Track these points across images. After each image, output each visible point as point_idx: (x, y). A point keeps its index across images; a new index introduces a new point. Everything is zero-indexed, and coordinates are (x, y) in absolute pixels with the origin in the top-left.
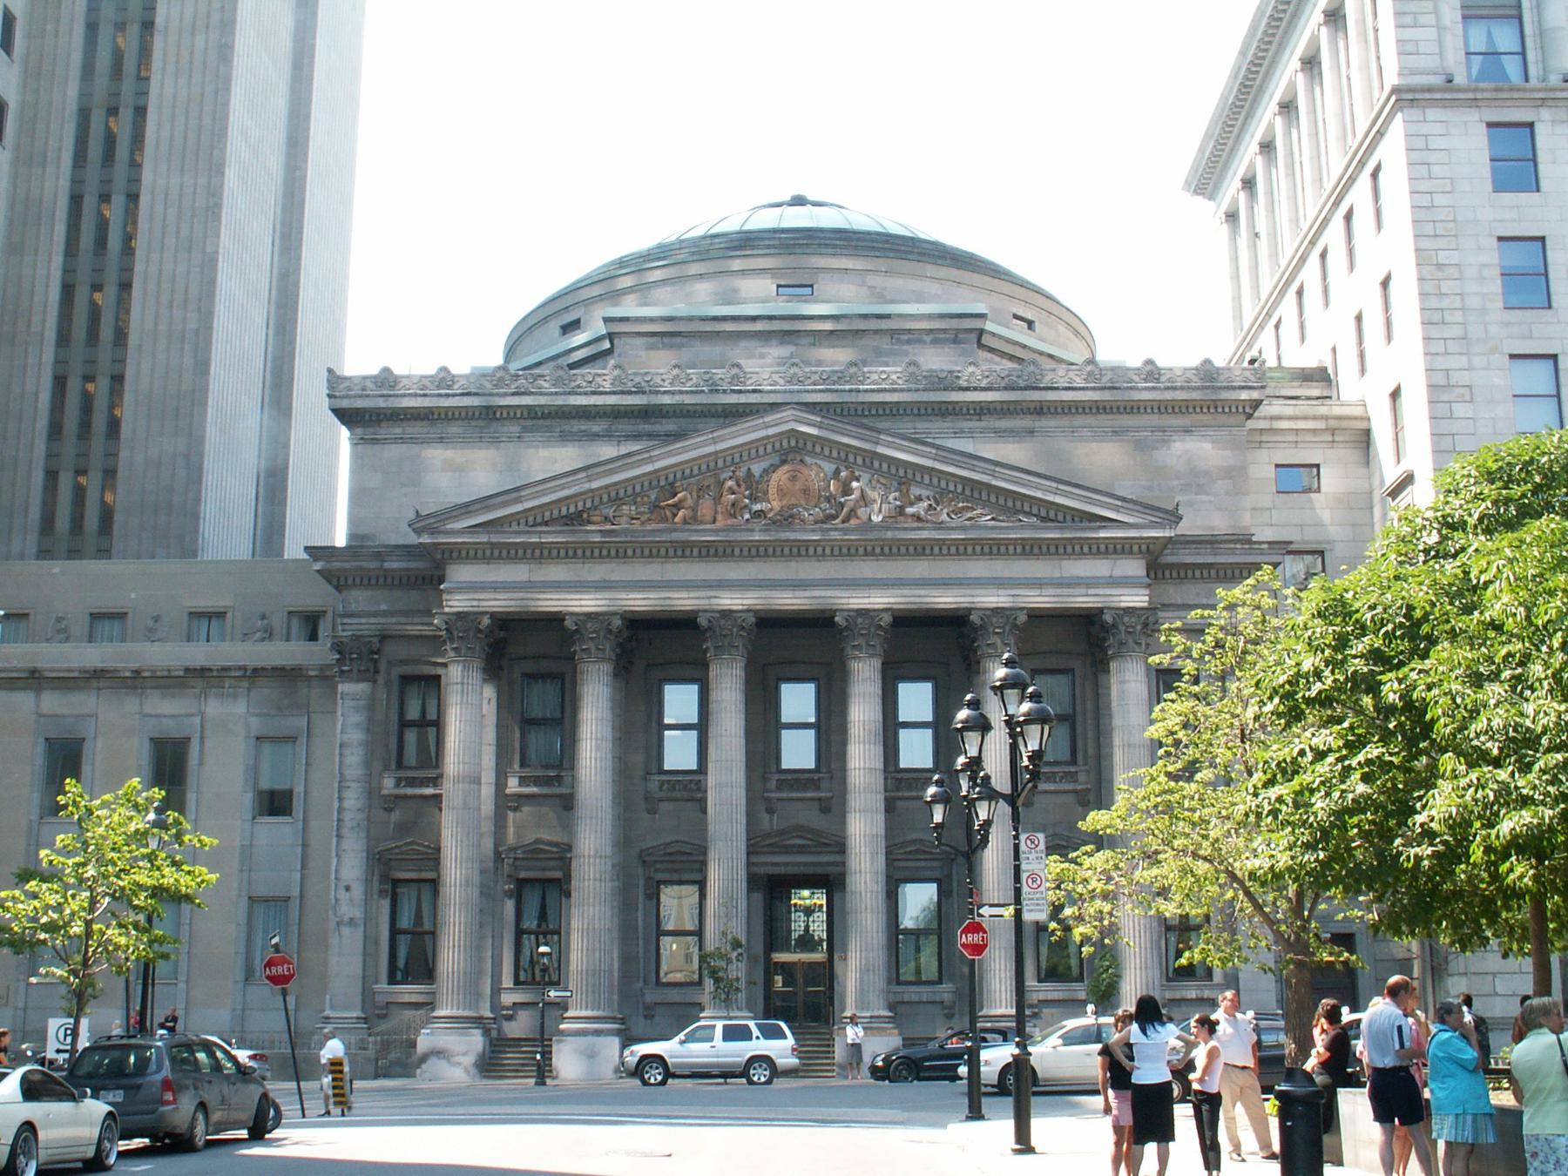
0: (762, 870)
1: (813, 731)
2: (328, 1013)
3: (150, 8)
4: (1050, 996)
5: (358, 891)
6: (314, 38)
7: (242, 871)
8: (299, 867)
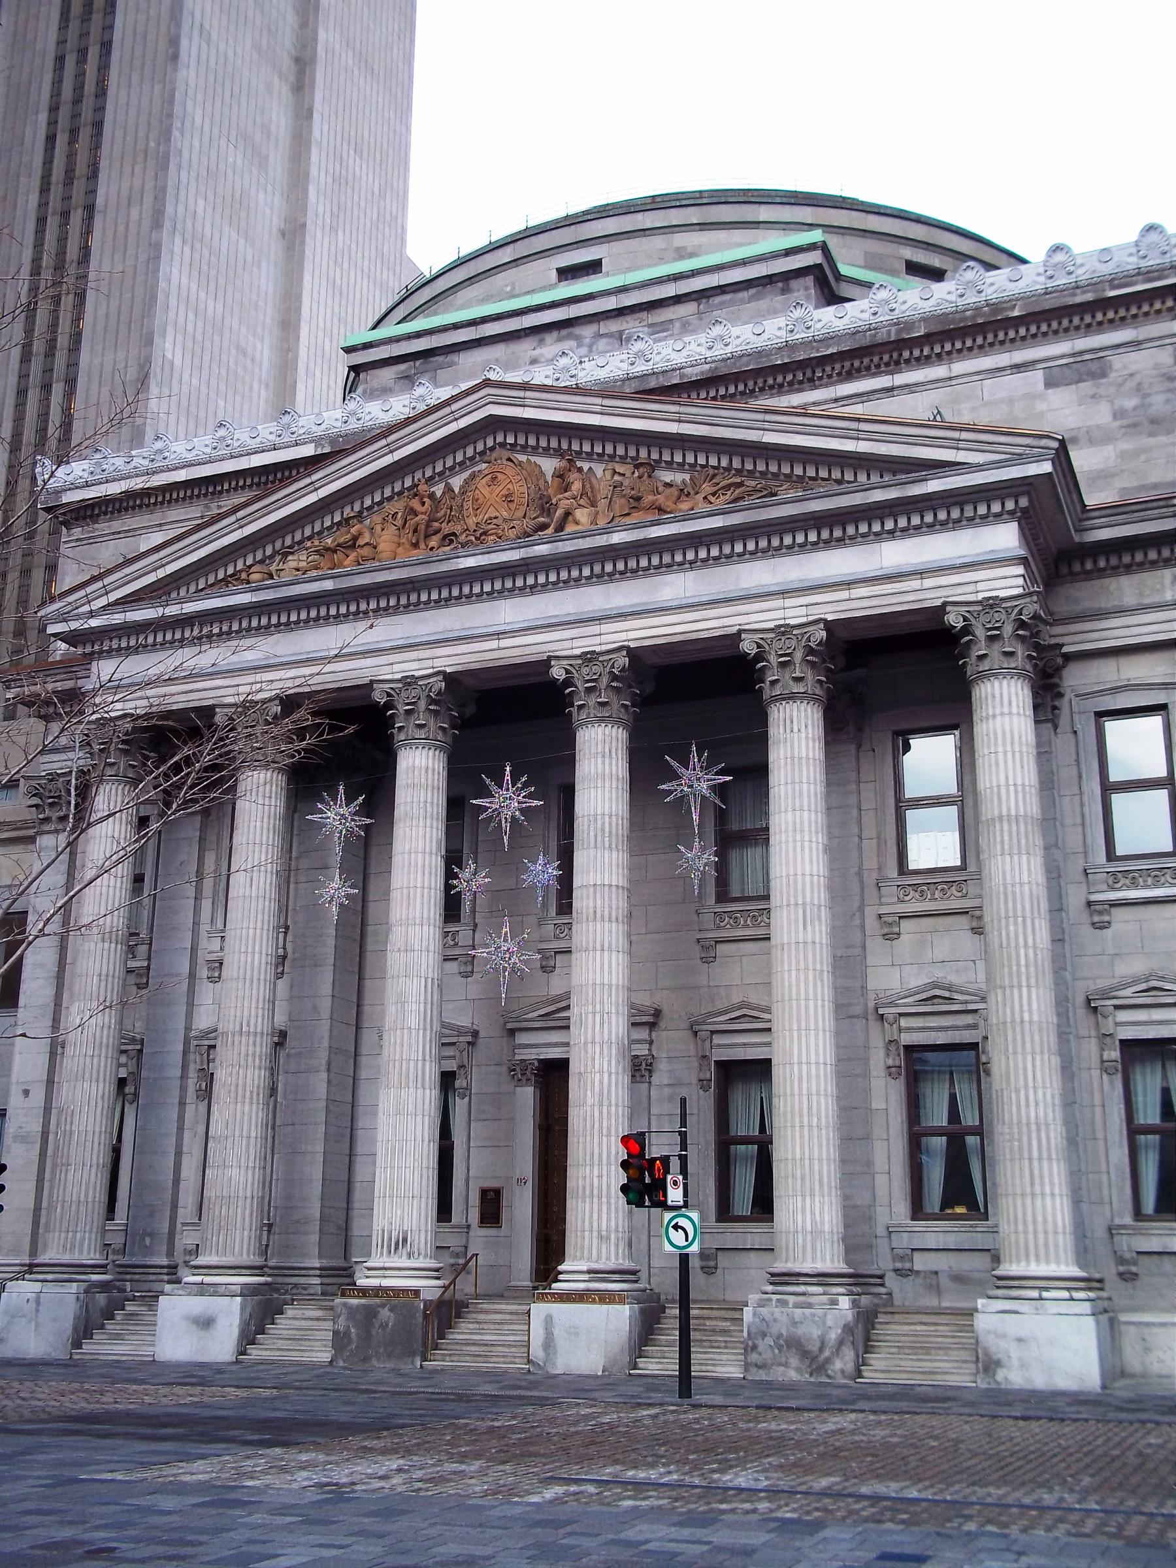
4: (931, 1241)
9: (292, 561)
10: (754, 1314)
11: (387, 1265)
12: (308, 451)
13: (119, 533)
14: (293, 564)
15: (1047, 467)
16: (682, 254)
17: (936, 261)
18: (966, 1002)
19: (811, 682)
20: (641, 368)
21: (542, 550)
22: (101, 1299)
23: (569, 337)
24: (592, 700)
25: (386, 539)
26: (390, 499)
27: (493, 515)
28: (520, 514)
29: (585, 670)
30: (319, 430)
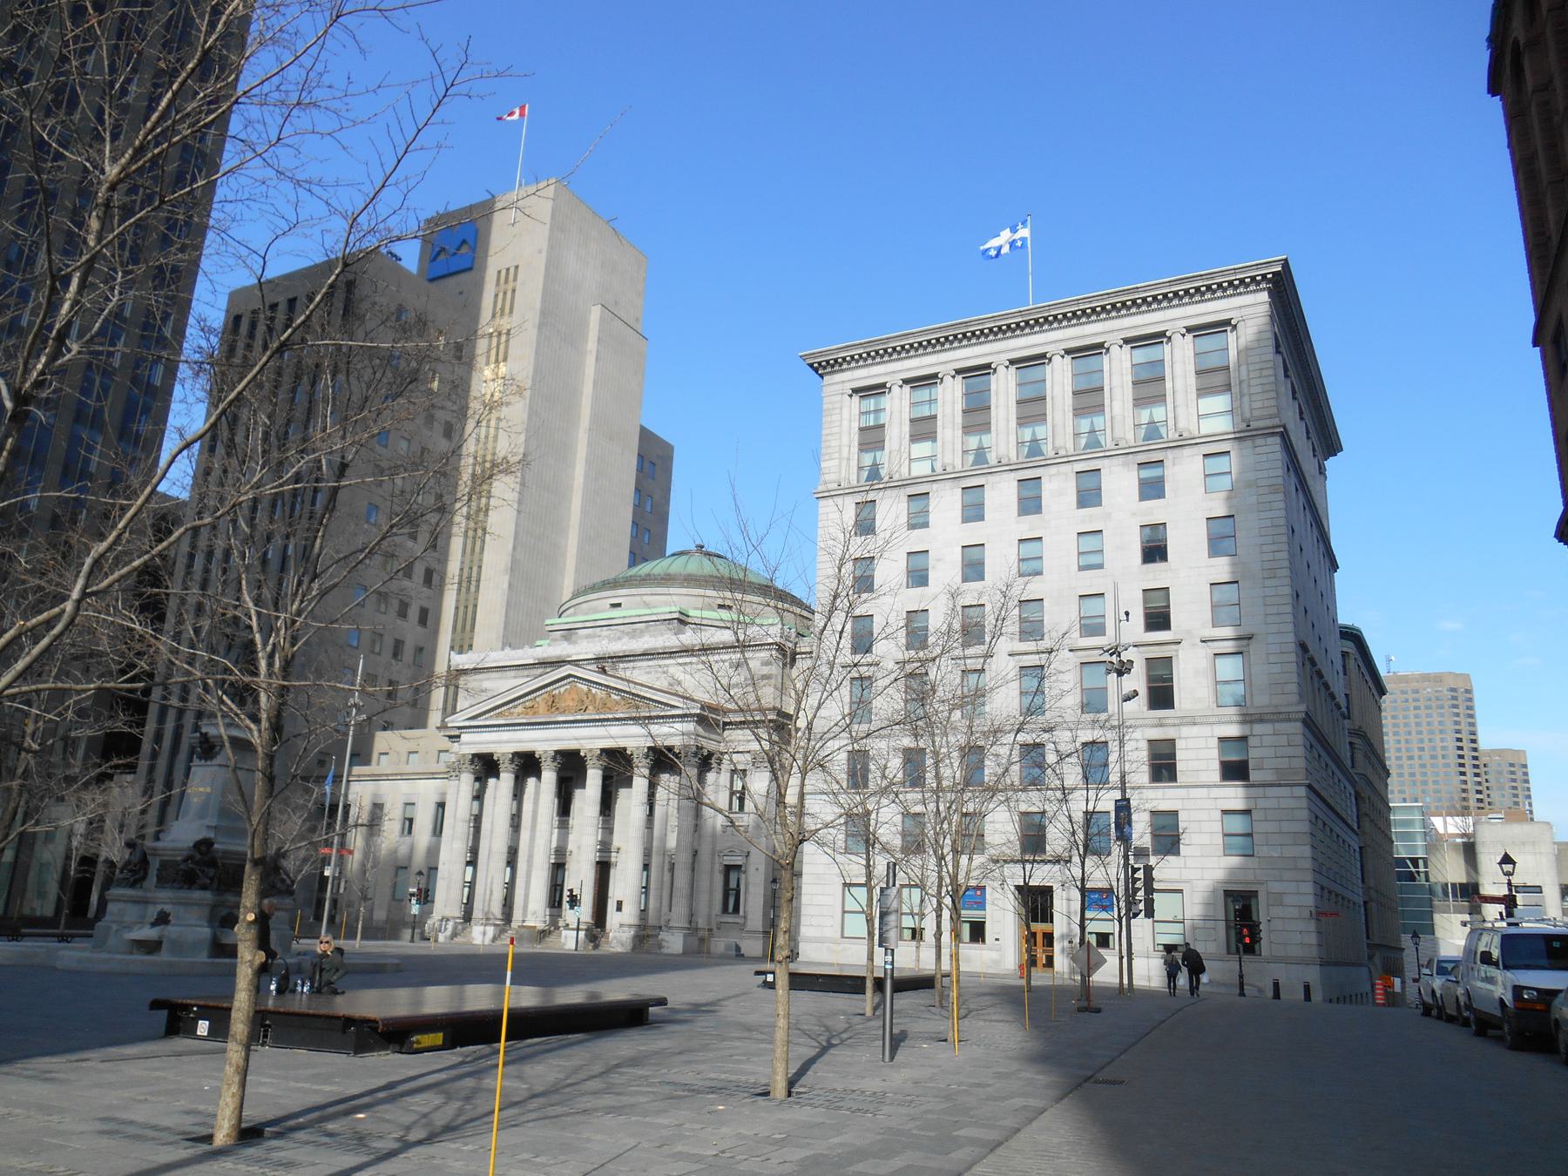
9: (516, 710)
15: (698, 711)
19: (645, 762)
20: (625, 648)
21: (579, 717)
22: (460, 927)
24: (591, 762)
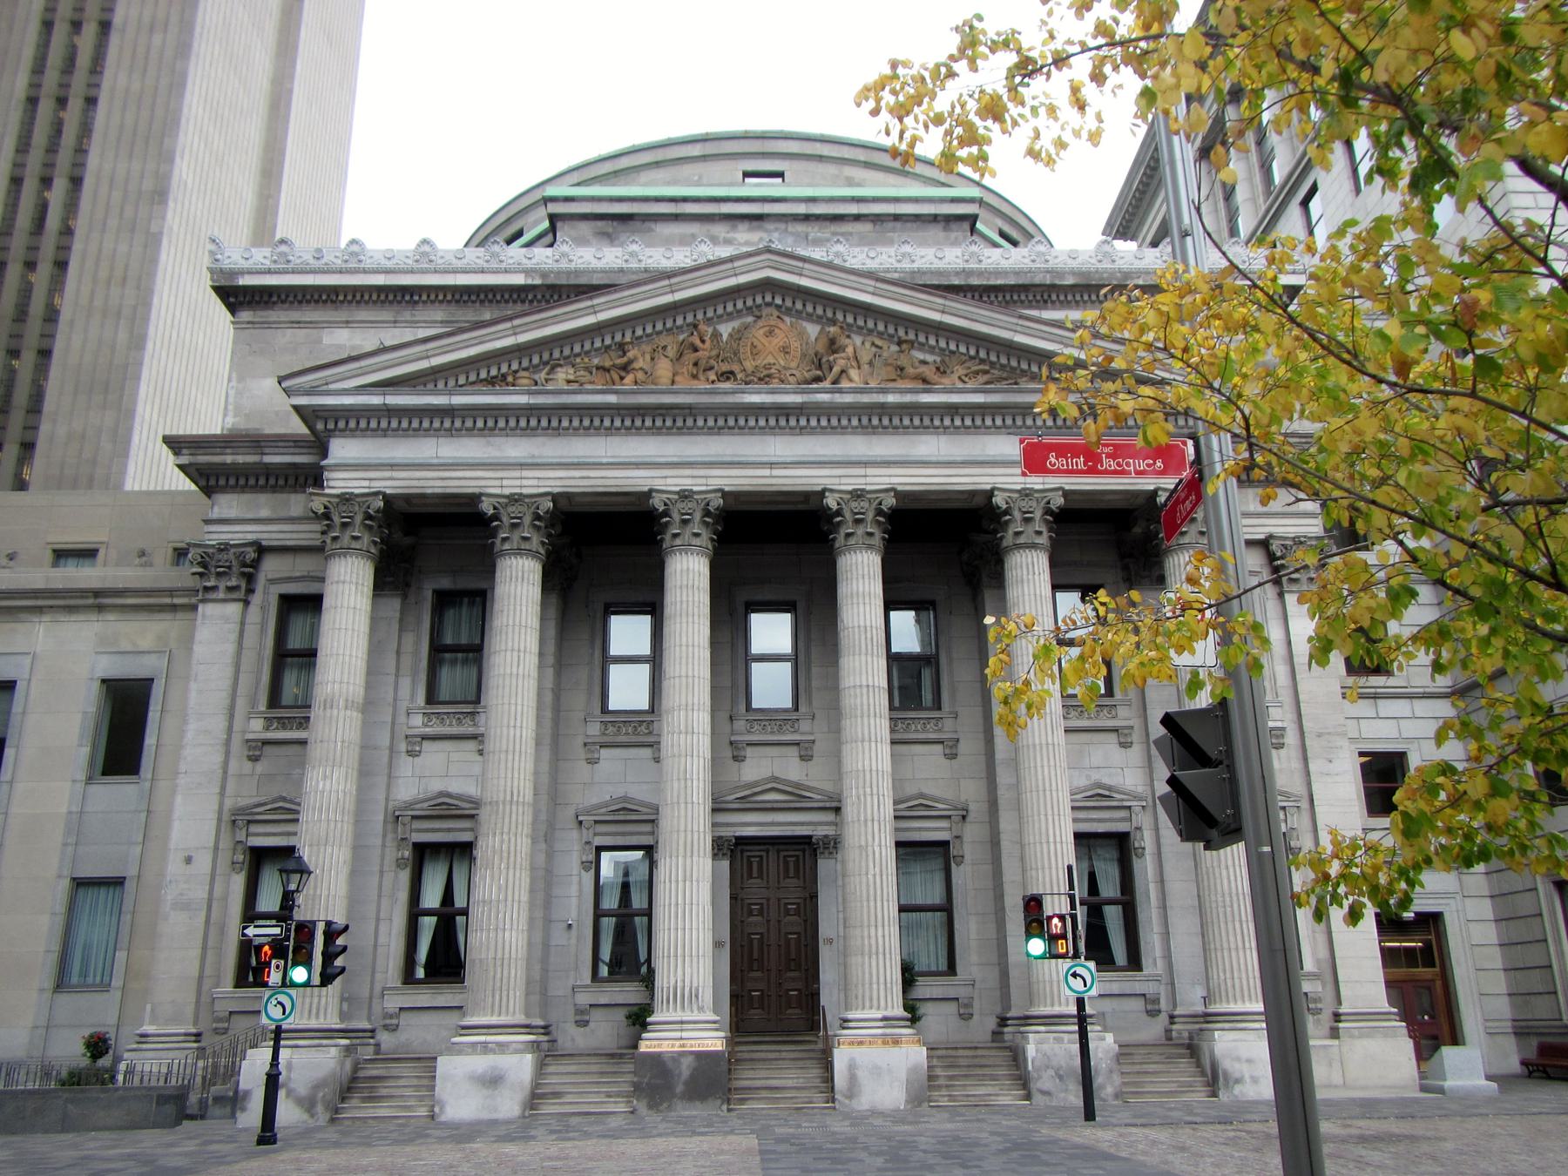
0: (728, 832)
1: (789, 664)
2: (149, 1028)
3: (109, 9)
5: (203, 863)
6: (292, 83)
7: (65, 845)
8: (140, 839)
9: (562, 374)
10: (1037, 1051)
11: (684, 1019)
12: (518, 280)
13: (299, 322)
14: (564, 376)
16: (850, 182)
17: (1014, 234)
18: (1123, 800)
23: (759, 228)
24: (860, 530)
25: (664, 369)
26: (659, 333)
27: (772, 361)
28: (794, 365)
29: (854, 504)
30: (529, 264)
